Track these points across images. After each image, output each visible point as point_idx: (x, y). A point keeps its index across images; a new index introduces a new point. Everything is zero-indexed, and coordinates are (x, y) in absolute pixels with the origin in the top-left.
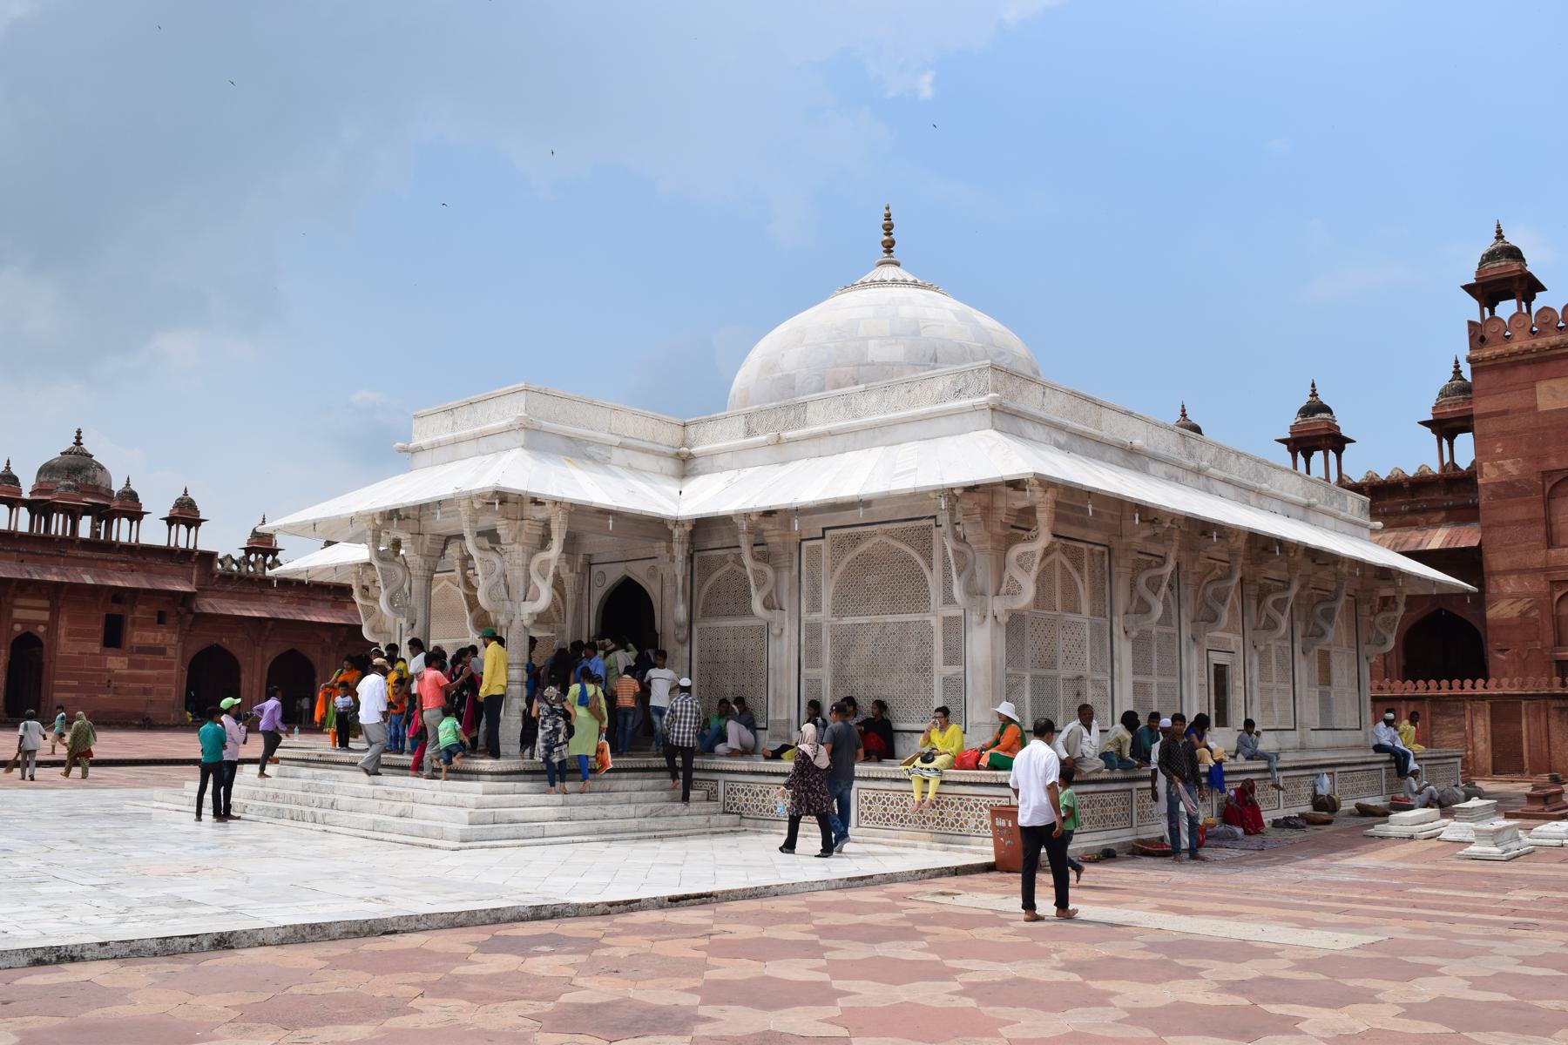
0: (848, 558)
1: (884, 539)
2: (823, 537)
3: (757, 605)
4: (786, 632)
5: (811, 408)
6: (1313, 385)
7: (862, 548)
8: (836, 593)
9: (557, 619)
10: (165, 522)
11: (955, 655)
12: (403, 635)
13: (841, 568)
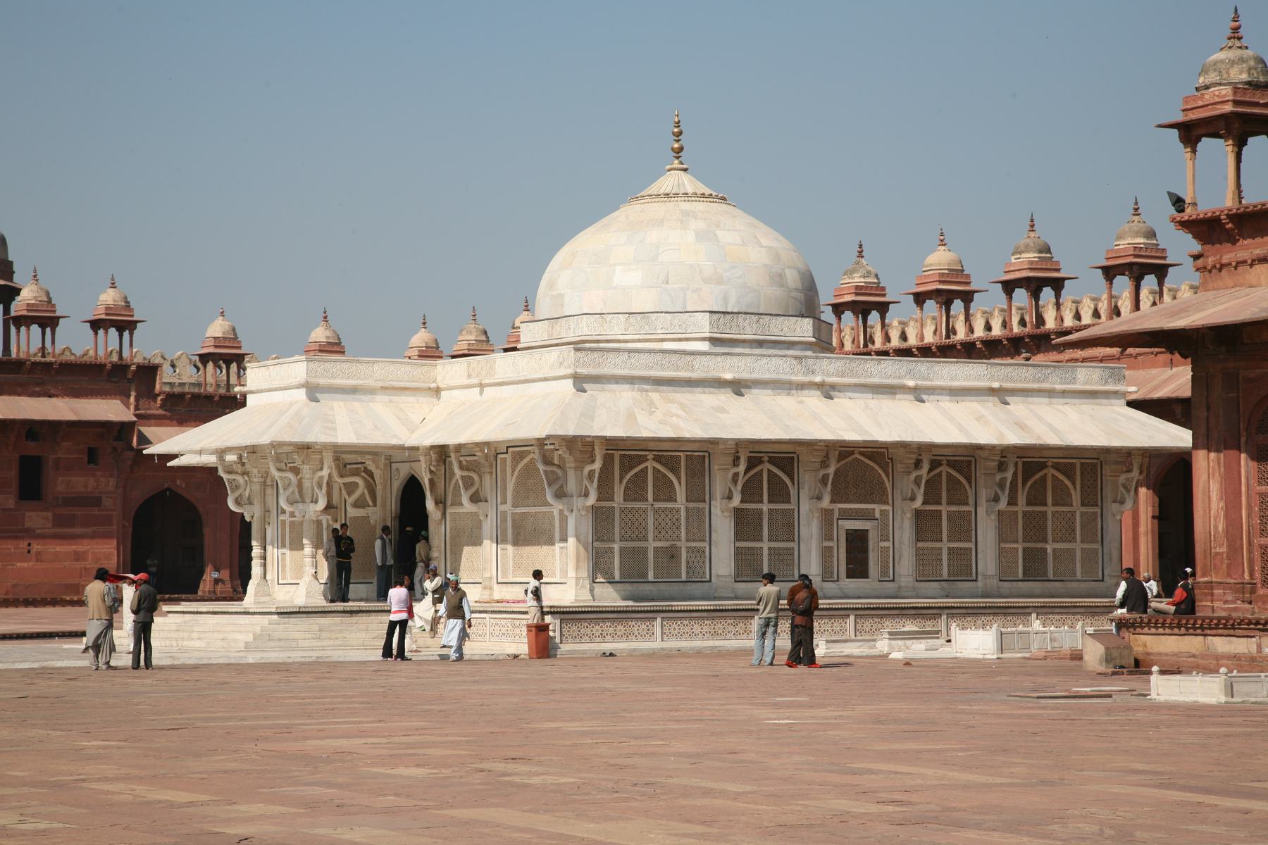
2: (507, 453)
3: (465, 500)
4: (489, 516)
9: (371, 503)
10: (88, 324)
13: (516, 474)
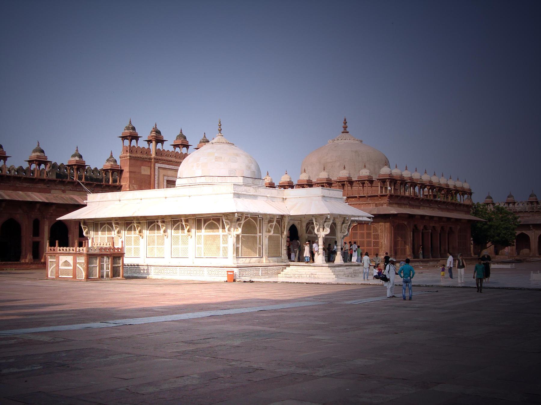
6: (77, 148)
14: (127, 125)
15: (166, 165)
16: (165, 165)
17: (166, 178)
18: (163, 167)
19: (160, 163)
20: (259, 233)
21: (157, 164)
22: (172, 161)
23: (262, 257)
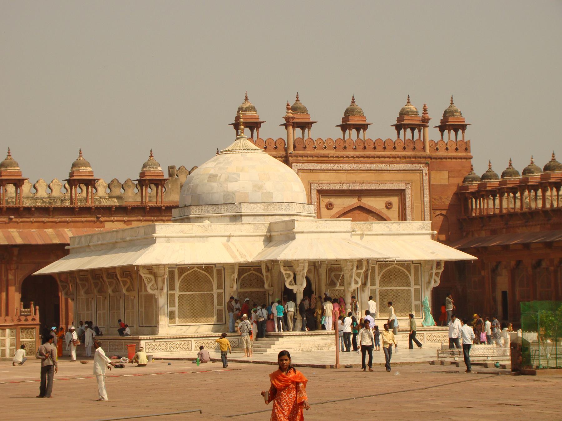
0: (385, 270)
1: (396, 266)
5: (374, 224)
6: (151, 151)
7: (389, 268)
8: (380, 280)
11: (418, 298)
12: (168, 289)
14: (240, 105)
15: (315, 164)
16: (313, 164)
17: (315, 187)
18: (308, 168)
19: (303, 163)
20: (218, 288)
21: (296, 164)
22: (328, 157)
23: (225, 324)
